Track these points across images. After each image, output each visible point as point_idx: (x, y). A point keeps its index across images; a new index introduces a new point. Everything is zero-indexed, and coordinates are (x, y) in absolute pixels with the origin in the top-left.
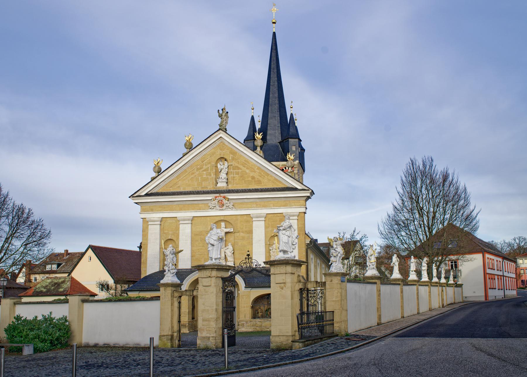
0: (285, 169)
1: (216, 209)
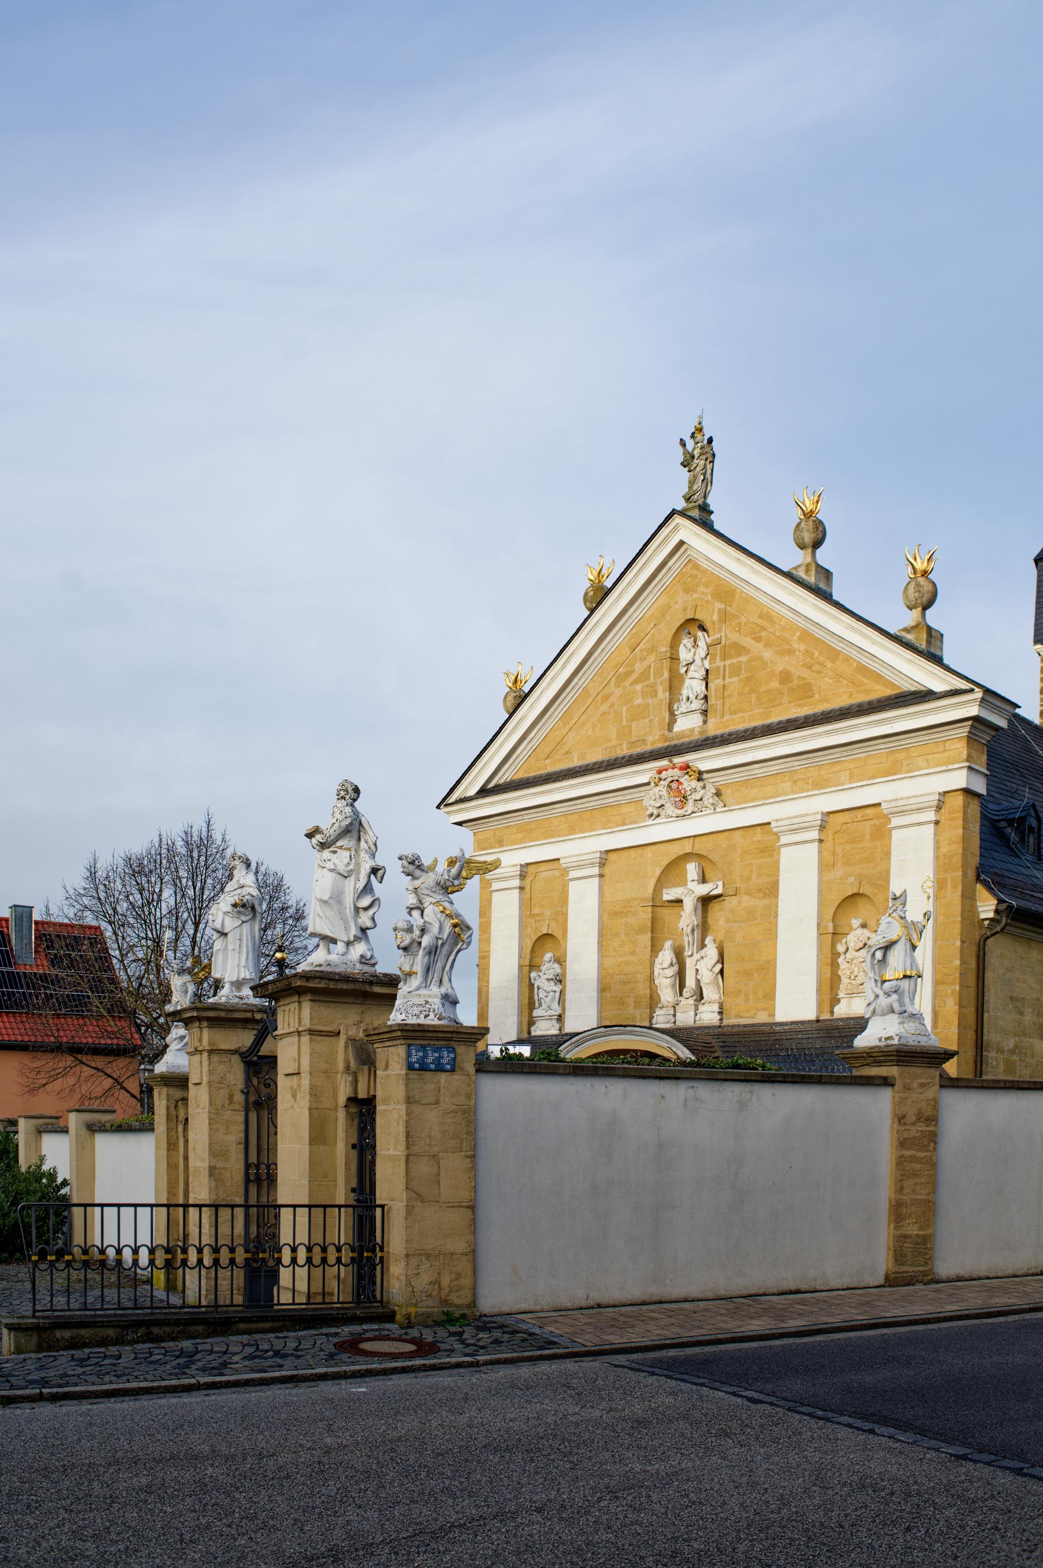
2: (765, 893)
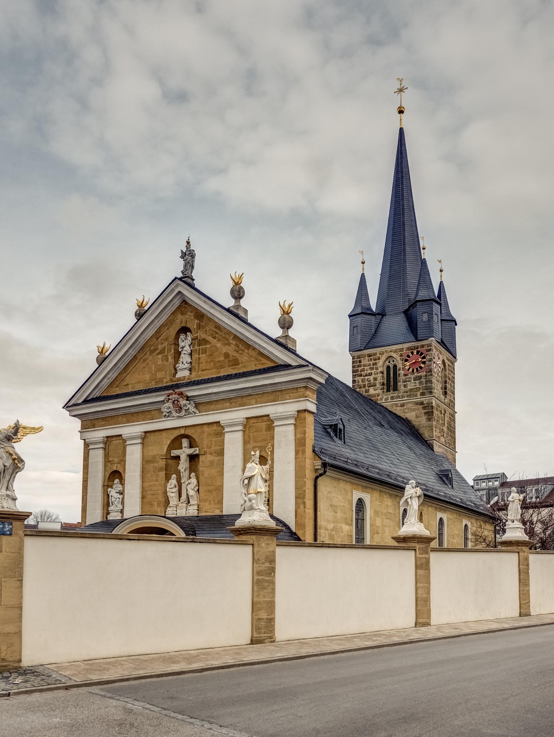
0: (411, 355)
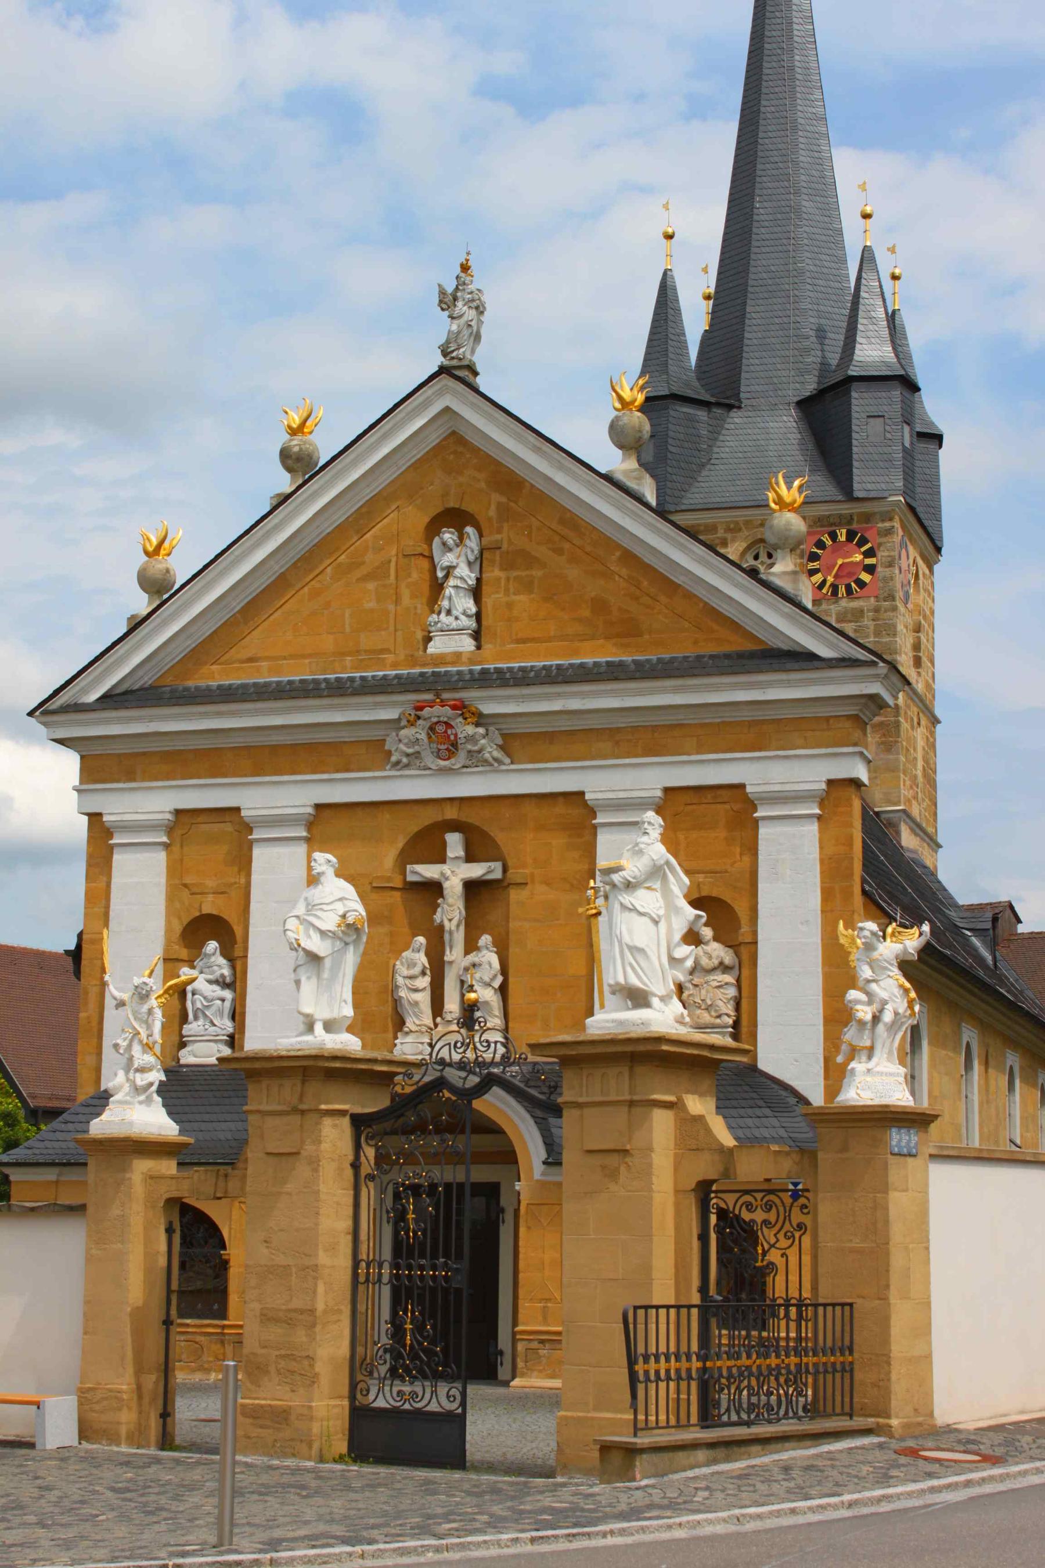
1: (419, 768)
2: (572, 885)
